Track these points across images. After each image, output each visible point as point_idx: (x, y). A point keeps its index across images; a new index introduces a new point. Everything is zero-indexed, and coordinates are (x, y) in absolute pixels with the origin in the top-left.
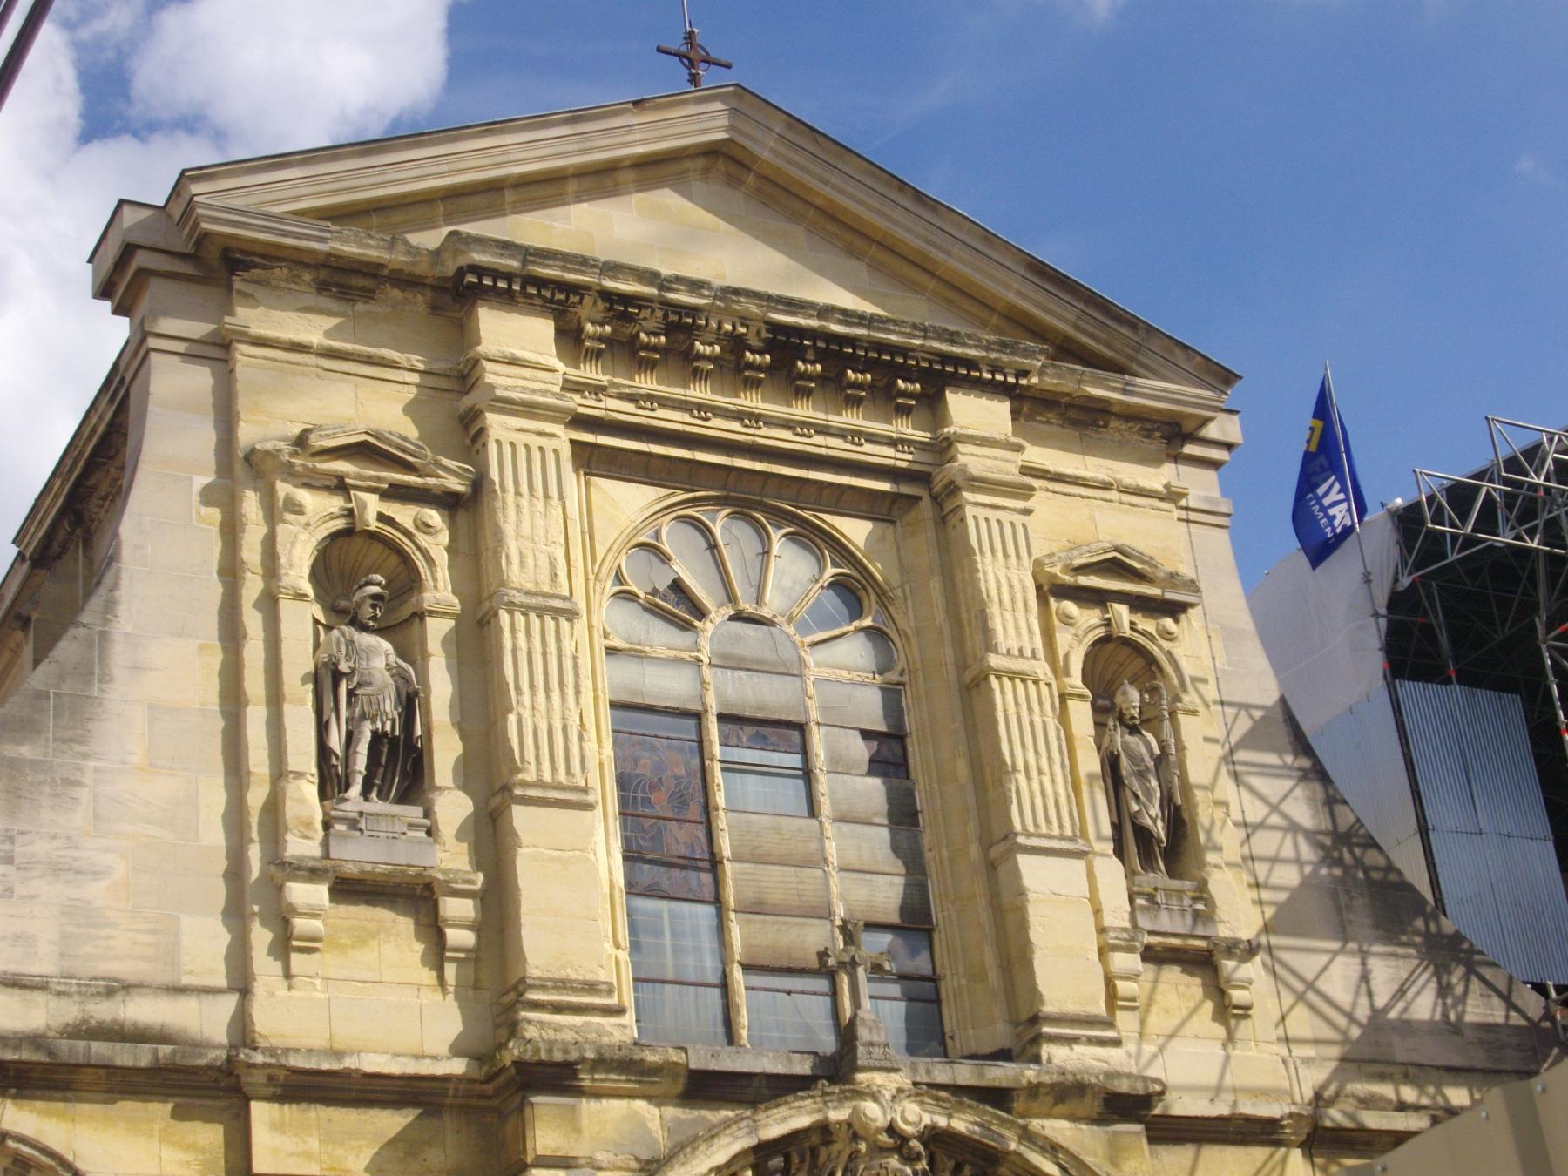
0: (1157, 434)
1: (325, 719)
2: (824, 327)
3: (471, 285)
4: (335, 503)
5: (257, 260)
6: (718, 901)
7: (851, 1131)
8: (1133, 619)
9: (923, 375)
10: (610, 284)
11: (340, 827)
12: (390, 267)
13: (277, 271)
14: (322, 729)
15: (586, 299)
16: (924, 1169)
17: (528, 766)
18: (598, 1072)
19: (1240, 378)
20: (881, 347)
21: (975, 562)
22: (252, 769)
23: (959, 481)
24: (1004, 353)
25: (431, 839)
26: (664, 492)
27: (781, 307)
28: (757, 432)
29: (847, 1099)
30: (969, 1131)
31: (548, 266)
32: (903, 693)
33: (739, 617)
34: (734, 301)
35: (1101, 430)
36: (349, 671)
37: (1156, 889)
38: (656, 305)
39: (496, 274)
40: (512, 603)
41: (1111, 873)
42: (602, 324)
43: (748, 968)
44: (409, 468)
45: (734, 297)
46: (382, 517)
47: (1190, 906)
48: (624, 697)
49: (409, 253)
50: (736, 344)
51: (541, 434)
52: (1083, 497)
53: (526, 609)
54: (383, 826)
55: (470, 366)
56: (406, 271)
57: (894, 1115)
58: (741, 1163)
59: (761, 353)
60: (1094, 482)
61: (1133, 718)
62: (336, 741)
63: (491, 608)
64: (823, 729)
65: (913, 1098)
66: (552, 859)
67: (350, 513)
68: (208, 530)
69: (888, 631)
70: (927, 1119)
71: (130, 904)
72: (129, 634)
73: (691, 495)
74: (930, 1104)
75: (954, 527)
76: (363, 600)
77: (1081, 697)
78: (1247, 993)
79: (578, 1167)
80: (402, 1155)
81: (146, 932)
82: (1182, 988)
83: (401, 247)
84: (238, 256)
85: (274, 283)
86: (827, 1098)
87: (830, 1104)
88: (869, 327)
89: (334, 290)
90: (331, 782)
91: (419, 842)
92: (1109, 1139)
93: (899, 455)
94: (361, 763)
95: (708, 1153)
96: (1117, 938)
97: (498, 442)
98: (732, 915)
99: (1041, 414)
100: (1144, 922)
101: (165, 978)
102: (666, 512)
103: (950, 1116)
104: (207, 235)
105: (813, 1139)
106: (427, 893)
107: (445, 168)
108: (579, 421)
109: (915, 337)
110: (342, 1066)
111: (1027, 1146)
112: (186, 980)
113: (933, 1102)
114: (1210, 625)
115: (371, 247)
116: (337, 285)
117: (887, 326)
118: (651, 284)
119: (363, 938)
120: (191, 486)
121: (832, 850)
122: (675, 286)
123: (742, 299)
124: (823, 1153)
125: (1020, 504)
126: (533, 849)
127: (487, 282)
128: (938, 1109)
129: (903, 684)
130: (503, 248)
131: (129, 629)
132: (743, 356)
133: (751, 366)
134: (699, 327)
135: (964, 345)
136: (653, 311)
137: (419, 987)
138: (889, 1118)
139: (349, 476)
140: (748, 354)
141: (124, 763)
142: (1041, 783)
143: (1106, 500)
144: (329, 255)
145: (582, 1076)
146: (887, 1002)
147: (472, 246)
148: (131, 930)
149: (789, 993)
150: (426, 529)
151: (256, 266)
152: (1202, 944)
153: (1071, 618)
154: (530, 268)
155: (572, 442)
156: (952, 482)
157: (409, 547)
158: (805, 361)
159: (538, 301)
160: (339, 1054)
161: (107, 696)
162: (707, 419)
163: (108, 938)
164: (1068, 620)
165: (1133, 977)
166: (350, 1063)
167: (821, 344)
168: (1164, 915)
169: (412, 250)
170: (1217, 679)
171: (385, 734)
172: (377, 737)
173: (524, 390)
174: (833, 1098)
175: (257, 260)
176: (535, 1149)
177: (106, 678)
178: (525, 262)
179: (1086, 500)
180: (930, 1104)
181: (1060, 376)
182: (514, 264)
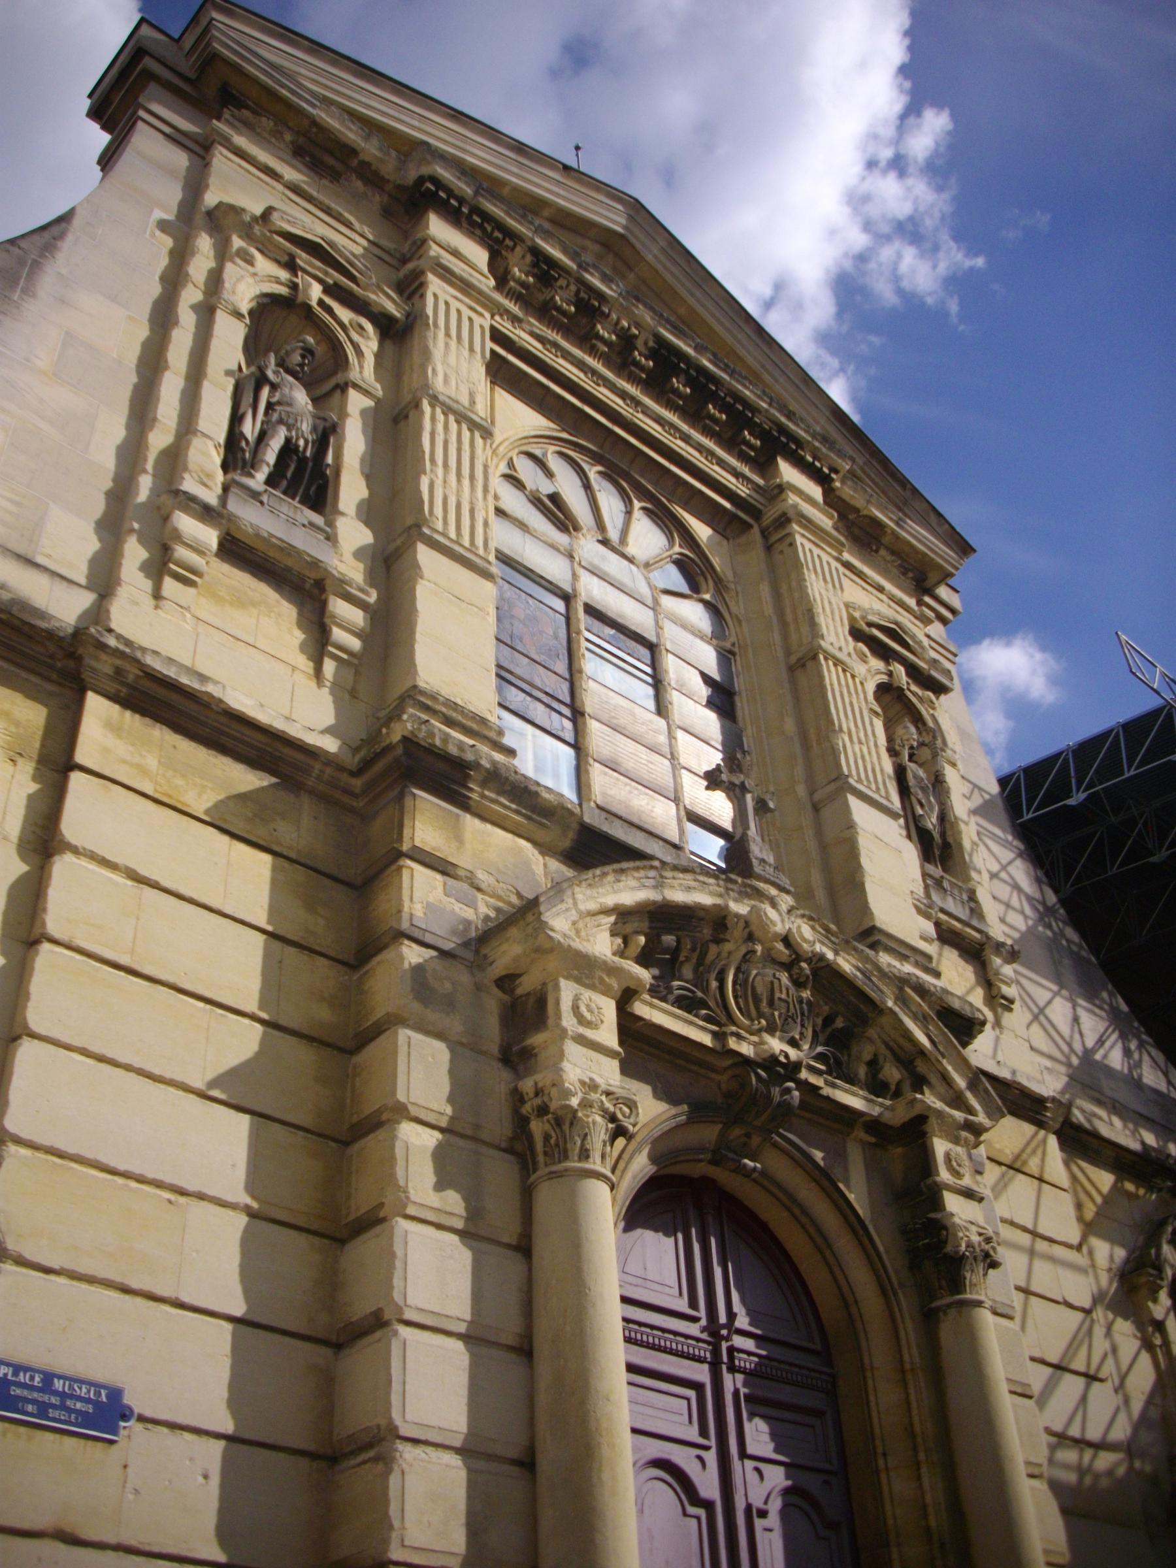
0: (910, 575)
1: (241, 411)
2: (698, 359)
7: (747, 930)
9: (764, 435)
13: (264, 119)
14: (236, 419)
15: (518, 249)
18: (489, 790)
19: (974, 551)
21: (803, 574)
22: (159, 416)
23: (791, 514)
26: (552, 425)
27: (669, 327)
28: (635, 413)
31: (495, 205)
34: (634, 305)
38: (572, 280)
39: (450, 193)
46: (321, 303)
50: (627, 341)
51: (471, 308)
52: (864, 589)
53: (448, 410)
56: (373, 167)
57: (791, 926)
62: (249, 429)
63: (414, 398)
67: (294, 287)
70: (818, 948)
75: (781, 552)
76: (297, 347)
79: (456, 877)
80: (250, 815)
82: (960, 969)
84: (234, 92)
85: (258, 130)
86: (730, 886)
87: (731, 893)
88: (731, 376)
89: (307, 159)
94: (271, 456)
97: (435, 295)
101: (21, 549)
102: (552, 442)
103: (836, 953)
105: (705, 931)
106: (316, 591)
108: (497, 336)
110: (203, 689)
112: (40, 559)
115: (351, 130)
116: (312, 156)
117: (744, 381)
119: (241, 602)
122: (591, 270)
124: (713, 949)
128: (826, 941)
133: (637, 364)
134: (603, 313)
135: (798, 425)
136: (568, 286)
137: (294, 668)
138: (787, 928)
142: (861, 750)
145: (471, 786)
151: (247, 107)
154: (481, 199)
156: (784, 514)
157: (342, 336)
159: (478, 232)
160: (203, 678)
162: (598, 385)
166: (210, 688)
168: (950, 899)
172: (289, 449)
174: (735, 887)
175: (250, 103)
176: (412, 839)
181: (855, 490)
182: (468, 190)
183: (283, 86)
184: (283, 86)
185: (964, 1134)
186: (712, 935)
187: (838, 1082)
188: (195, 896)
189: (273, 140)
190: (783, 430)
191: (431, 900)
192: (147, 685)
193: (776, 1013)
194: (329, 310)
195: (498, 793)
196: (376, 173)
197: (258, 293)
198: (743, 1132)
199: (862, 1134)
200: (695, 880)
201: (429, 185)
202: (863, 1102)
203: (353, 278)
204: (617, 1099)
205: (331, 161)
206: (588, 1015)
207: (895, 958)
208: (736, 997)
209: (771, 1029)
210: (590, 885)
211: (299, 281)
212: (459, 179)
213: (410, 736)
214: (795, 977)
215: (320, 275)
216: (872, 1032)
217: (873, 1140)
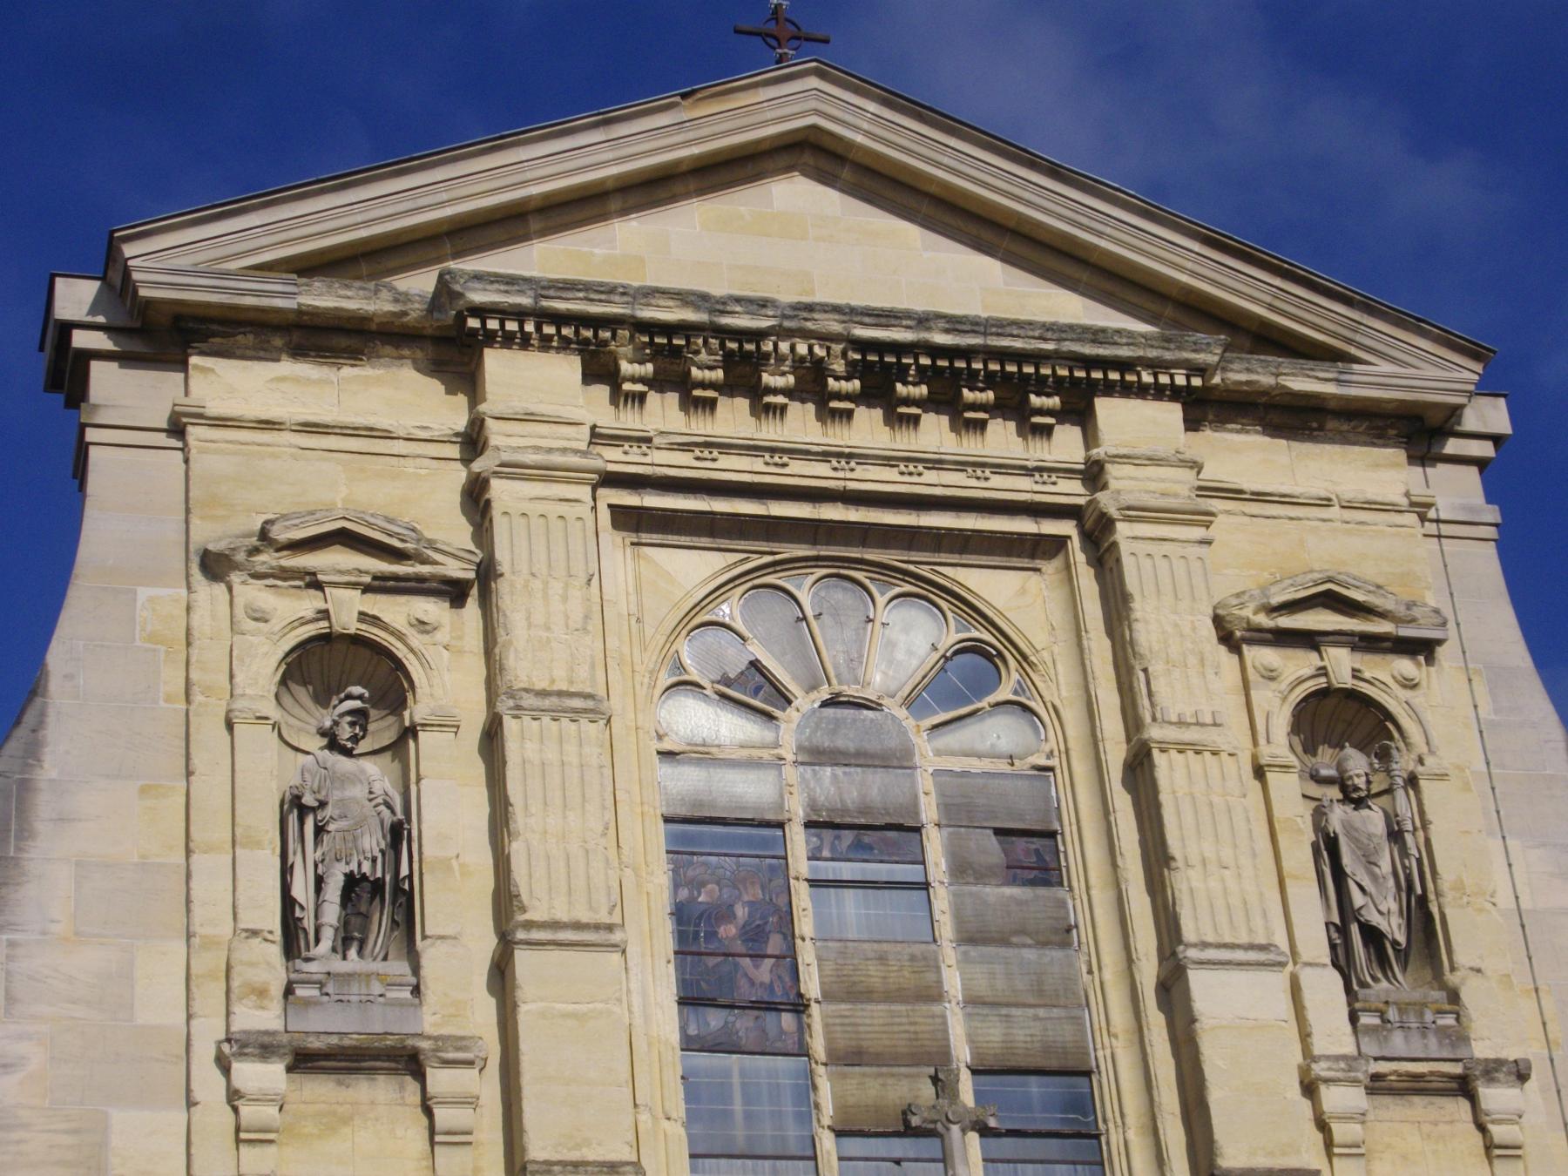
0: (1392, 432)
3: (474, 331)
4: (309, 603)
5: (215, 327)
6: (803, 1051)
8: (1357, 666)
10: (647, 314)
11: (301, 992)
12: (377, 320)
13: (240, 337)
14: (286, 871)
17: (538, 903)
20: (1004, 355)
23: (1113, 512)
24: (1168, 349)
25: (417, 1001)
26: (733, 558)
28: (849, 475)
32: (1052, 779)
33: (832, 702)
34: (806, 319)
35: (1315, 433)
36: (316, 804)
37: (1387, 1003)
39: (503, 313)
40: (518, 707)
41: (1325, 989)
42: (641, 363)
43: (839, 1133)
44: (398, 555)
45: (805, 315)
46: (363, 617)
47: (1434, 1022)
48: (683, 812)
49: (396, 301)
52: (1291, 519)
54: (355, 989)
55: (477, 429)
59: (848, 379)
60: (1306, 498)
61: (1357, 789)
64: (946, 831)
66: (566, 1015)
68: (154, 650)
69: (1032, 704)
71: (47, 1101)
72: (54, 780)
73: (768, 559)
77: (1285, 768)
78: (1516, 1127)
81: (66, 1132)
82: (1426, 1128)
83: (385, 294)
84: (191, 325)
88: (985, 334)
90: (293, 938)
91: (400, 1003)
94: (332, 912)
96: (1329, 1069)
98: (821, 1070)
100: (1370, 1048)
102: (737, 582)
104: (149, 302)
107: (445, 196)
109: (1045, 340)
114: (1471, 666)
118: (697, 308)
119: (335, 1122)
120: (135, 600)
121: (953, 981)
122: (729, 308)
123: (816, 316)
125: (1198, 533)
126: (544, 1004)
127: (493, 324)
129: (1051, 769)
130: (507, 283)
131: (54, 774)
132: (826, 384)
134: (767, 356)
139: (323, 572)
140: (831, 381)
141: (44, 933)
143: (1324, 520)
144: (300, 312)
146: (1030, 1166)
148: (49, 1131)
149: (898, 1162)
150: (422, 627)
151: (214, 335)
153: (1272, 671)
155: (610, 506)
157: (400, 651)
158: (905, 383)
161: (26, 855)
162: (784, 465)
163: (19, 1142)
164: (1271, 676)
165: (1361, 1117)
167: (925, 361)
169: (400, 297)
170: (1481, 732)
172: (352, 883)
173: (537, 449)
177: (25, 833)
178: (538, 297)
179: (1295, 522)
181: (1248, 370)
182: (525, 301)
190: (1090, 363)
194: (375, 620)
197: (281, 654)
201: (473, 323)
205: (343, 342)
211: (330, 606)
215: (353, 579)
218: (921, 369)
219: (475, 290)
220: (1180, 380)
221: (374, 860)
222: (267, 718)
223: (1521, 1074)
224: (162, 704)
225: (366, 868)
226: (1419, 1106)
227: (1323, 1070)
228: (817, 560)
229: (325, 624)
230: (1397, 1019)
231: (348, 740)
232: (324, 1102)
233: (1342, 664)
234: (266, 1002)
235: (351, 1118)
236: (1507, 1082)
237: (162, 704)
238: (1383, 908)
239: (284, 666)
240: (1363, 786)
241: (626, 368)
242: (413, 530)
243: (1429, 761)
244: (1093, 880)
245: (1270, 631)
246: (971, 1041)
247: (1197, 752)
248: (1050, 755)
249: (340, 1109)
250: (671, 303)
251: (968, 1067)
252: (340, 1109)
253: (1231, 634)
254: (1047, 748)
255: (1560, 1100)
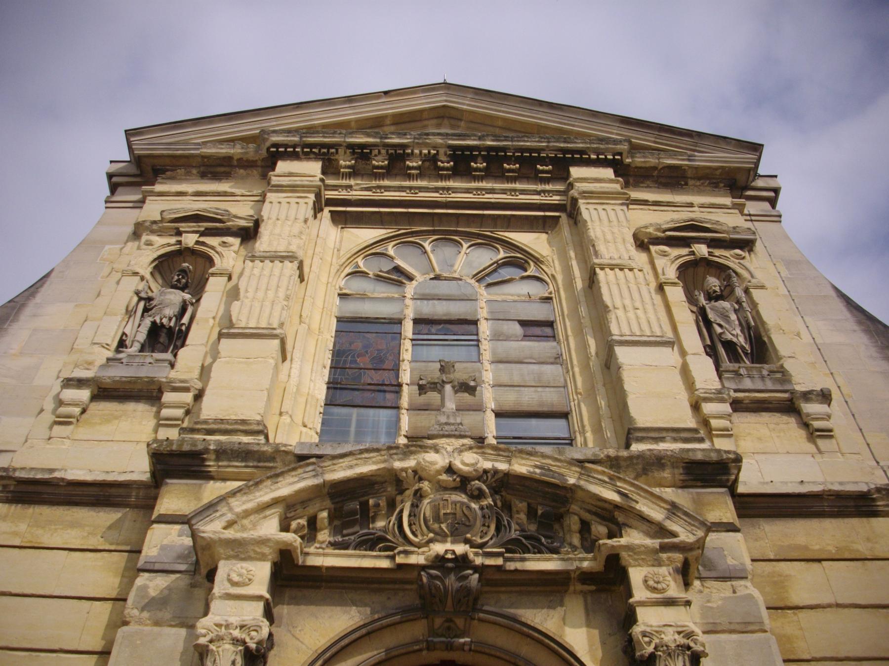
0: (722, 185)
2: (484, 144)
6: (397, 408)
7: (417, 477)
8: (710, 250)
9: (554, 161)
12: (235, 158)
13: (178, 171)
15: (340, 150)
16: (489, 504)
18: (223, 461)
20: (522, 150)
24: (602, 144)
27: (455, 138)
29: (412, 453)
30: (529, 472)
31: (314, 137)
34: (426, 139)
35: (684, 187)
39: (286, 146)
40: (253, 256)
45: (425, 137)
47: (768, 375)
50: (432, 160)
52: (674, 211)
56: (245, 159)
57: (452, 460)
58: (318, 505)
65: (475, 450)
74: (492, 454)
77: (674, 284)
78: (828, 422)
82: (772, 426)
84: (158, 167)
87: (395, 457)
88: (512, 141)
89: (209, 175)
92: (693, 498)
93: (542, 198)
95: (272, 487)
99: (642, 183)
103: (509, 462)
105: (389, 489)
109: (542, 142)
111: (587, 481)
113: (495, 453)
116: (211, 173)
117: (523, 139)
122: (389, 136)
123: (430, 137)
128: (500, 458)
129: (551, 298)
130: (288, 133)
133: (443, 169)
134: (408, 155)
135: (575, 143)
136: (379, 152)
138: (447, 461)
145: (208, 463)
147: (271, 135)
150: (224, 245)
151: (168, 170)
152: (786, 395)
153: (665, 252)
154: (304, 139)
155: (330, 211)
159: (312, 156)
160: (52, 471)
166: (57, 475)
171: (162, 325)
178: (301, 137)
180: (492, 454)
181: (644, 157)
182: (296, 139)
183: (178, 150)
184: (178, 150)
185: (664, 556)
186: (396, 490)
187: (526, 555)
188: (34, 592)
189: (188, 177)
190: (564, 151)
191: (165, 542)
192: (22, 488)
193: (443, 526)
195: (230, 460)
196: (247, 161)
198: (444, 619)
199: (579, 587)
200: (356, 459)
202: (559, 563)
203: (220, 221)
204: (249, 628)
205: (222, 169)
206: (236, 578)
207: (651, 443)
208: (410, 525)
209: (441, 537)
210: (245, 493)
212: (288, 136)
213: (155, 452)
214: (469, 493)
216: (574, 508)
217: (593, 588)
218: (483, 156)
219: (273, 136)
220: (610, 157)
221: (170, 319)
222: (138, 273)
223: (825, 397)
224: (99, 279)
225: (165, 321)
226: (766, 417)
227: (701, 393)
228: (434, 232)
229: (178, 246)
230: (746, 373)
231: (176, 281)
232: (109, 410)
233: (702, 250)
234: (90, 367)
235: (121, 417)
236: (817, 401)
237: (99, 279)
238: (734, 332)
239: (157, 262)
240: (719, 291)
241: (342, 163)
242: (227, 211)
243: (753, 281)
244: (569, 333)
245: (662, 238)
246: (495, 400)
247: (621, 269)
248: (551, 293)
249: (116, 413)
250: (362, 136)
251: (493, 411)
252: (116, 413)
253: (643, 242)
254: (549, 291)
255: (855, 419)
